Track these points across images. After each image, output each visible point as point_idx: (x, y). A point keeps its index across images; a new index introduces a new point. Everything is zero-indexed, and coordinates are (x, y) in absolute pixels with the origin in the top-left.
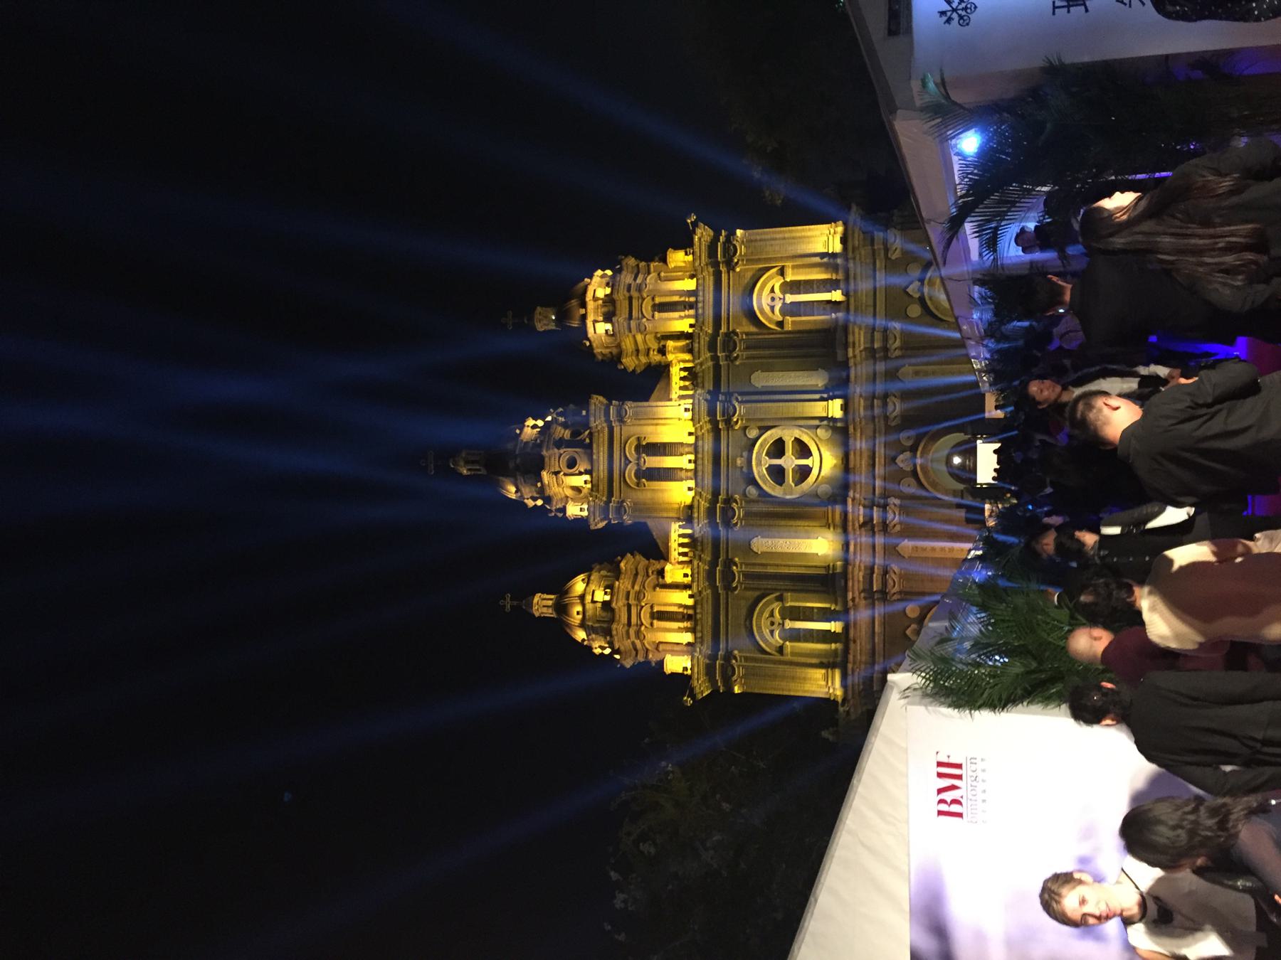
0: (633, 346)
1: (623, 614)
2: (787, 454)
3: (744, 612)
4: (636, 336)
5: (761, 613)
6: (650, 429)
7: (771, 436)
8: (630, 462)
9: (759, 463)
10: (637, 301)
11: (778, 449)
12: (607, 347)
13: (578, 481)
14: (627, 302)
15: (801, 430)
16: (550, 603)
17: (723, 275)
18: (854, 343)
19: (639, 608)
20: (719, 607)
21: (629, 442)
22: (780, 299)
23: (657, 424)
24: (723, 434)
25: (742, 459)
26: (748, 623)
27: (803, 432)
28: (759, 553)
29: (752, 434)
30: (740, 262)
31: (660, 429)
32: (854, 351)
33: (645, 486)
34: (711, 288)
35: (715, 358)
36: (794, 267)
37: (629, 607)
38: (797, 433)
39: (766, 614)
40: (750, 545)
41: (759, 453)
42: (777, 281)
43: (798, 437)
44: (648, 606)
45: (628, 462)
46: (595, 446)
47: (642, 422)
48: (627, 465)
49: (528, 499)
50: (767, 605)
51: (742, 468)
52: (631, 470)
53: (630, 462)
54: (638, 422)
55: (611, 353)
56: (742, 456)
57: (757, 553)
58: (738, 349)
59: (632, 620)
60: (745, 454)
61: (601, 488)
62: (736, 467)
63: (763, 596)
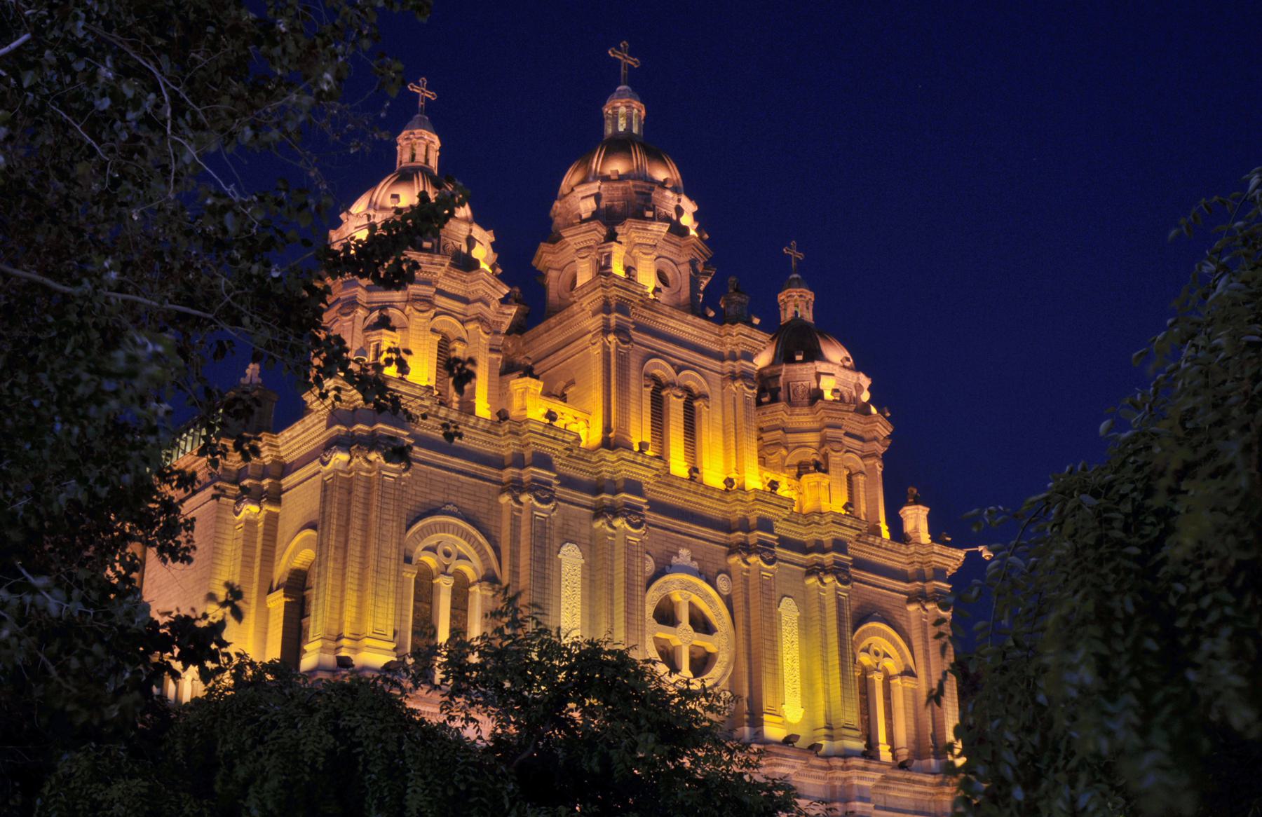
0: (795, 426)
1: (455, 285)
2: (696, 635)
3: (468, 505)
4: (814, 434)
5: (468, 537)
6: (718, 418)
7: (716, 612)
8: (677, 374)
9: (687, 587)
10: (860, 447)
11: (702, 624)
12: (788, 385)
13: (647, 280)
14: (858, 433)
15: (729, 664)
16: (420, 159)
17: (903, 584)
18: (865, 769)
19: (461, 317)
20: (476, 462)
21: (702, 380)
22: (877, 664)
23: (725, 432)
24: (720, 536)
25: (689, 559)
26: (450, 508)
27: (727, 667)
28: (560, 556)
29: (722, 581)
30: (924, 613)
31: (720, 434)
32: (857, 768)
33: (646, 386)
34: (889, 563)
35: (819, 547)
36: (915, 693)
37: (465, 300)
38: (723, 658)
39: (463, 546)
40: (571, 542)
41: (697, 591)
42: (896, 665)
43: (720, 657)
44: (464, 335)
45: (679, 369)
46: (698, 321)
47: (730, 409)
48: (673, 365)
49: (599, 188)
50: (481, 551)
51: (677, 555)
52: (662, 369)
53: (677, 374)
54: (729, 401)
55: (779, 389)
56: (693, 559)
57: (559, 552)
58: (839, 585)
59: (443, 299)
60: (695, 565)
61: (646, 313)
62: (679, 546)
63: (497, 549)
